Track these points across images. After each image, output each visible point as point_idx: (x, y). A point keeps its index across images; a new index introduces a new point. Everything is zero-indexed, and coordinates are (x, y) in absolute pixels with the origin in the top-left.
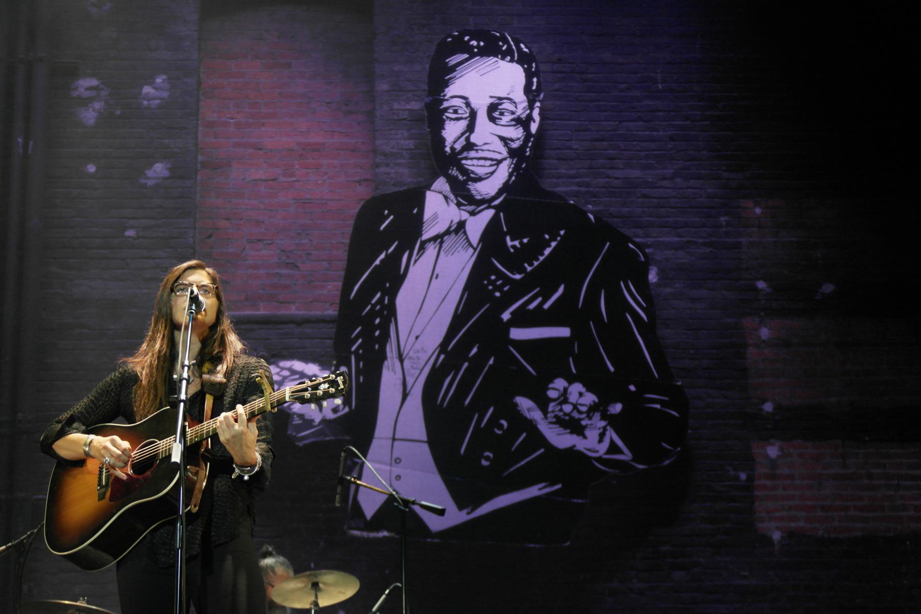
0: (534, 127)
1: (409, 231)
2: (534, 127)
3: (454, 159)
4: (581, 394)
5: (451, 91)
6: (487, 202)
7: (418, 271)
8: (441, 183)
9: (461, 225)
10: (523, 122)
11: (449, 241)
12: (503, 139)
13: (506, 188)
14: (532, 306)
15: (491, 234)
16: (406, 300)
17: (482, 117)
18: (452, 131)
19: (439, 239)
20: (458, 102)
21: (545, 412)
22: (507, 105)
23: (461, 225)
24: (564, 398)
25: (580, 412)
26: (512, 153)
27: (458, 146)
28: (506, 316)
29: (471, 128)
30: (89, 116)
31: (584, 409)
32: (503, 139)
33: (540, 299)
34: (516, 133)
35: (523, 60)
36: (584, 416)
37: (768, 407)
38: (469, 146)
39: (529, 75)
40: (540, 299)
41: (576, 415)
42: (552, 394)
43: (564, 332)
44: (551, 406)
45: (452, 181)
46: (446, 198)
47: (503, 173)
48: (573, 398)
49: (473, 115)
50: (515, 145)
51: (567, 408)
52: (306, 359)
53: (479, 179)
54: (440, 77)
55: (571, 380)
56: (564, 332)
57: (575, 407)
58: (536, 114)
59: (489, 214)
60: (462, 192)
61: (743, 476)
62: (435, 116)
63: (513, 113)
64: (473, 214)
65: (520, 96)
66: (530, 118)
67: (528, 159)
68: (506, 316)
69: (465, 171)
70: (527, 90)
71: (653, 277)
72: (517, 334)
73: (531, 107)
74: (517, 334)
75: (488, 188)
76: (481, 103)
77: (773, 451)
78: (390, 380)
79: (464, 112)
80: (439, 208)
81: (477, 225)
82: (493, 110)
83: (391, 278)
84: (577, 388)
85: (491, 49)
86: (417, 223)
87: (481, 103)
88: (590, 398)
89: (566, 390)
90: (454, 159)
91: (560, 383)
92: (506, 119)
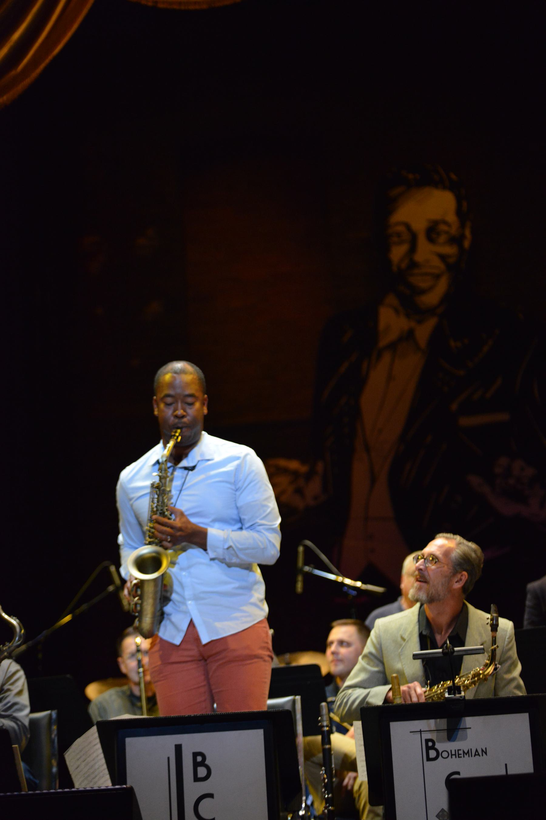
0: (467, 244)
2: (467, 244)
6: (431, 311)
7: (377, 376)
8: (392, 299)
16: (369, 399)
18: (398, 253)
19: (393, 346)
20: (401, 228)
22: (443, 227)
27: (404, 265)
28: (454, 407)
29: (413, 249)
34: (450, 250)
35: (452, 187)
38: (413, 265)
39: (459, 200)
46: (397, 311)
47: (442, 286)
49: (414, 238)
50: (451, 260)
52: (289, 457)
53: (423, 292)
58: (468, 233)
63: (447, 232)
64: (420, 322)
65: (452, 218)
66: (462, 237)
68: (454, 407)
70: (459, 212)
72: (465, 421)
73: (462, 226)
74: (465, 421)
75: (432, 299)
76: (420, 226)
80: (391, 320)
81: (424, 332)
82: (432, 232)
87: (420, 226)
92: (442, 238)
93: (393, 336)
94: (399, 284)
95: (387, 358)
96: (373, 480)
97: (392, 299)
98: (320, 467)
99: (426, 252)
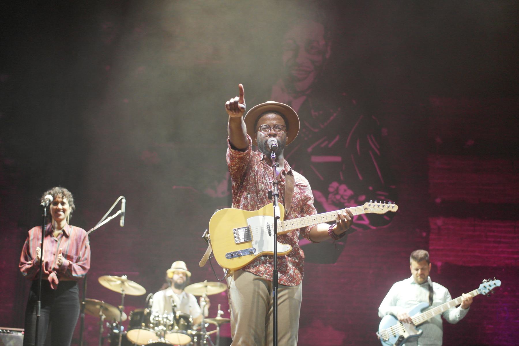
4: (345, 191)
14: (323, 145)
21: (327, 198)
24: (337, 192)
25: (345, 199)
28: (310, 150)
31: (346, 198)
33: (326, 142)
36: (346, 201)
37: (438, 200)
40: (326, 142)
41: (342, 200)
42: (331, 190)
43: (338, 159)
44: (330, 196)
48: (341, 192)
51: (338, 197)
55: (340, 183)
56: (338, 159)
57: (342, 197)
61: (424, 234)
68: (310, 150)
77: (440, 222)
84: (343, 187)
88: (349, 192)
89: (338, 188)
91: (335, 184)
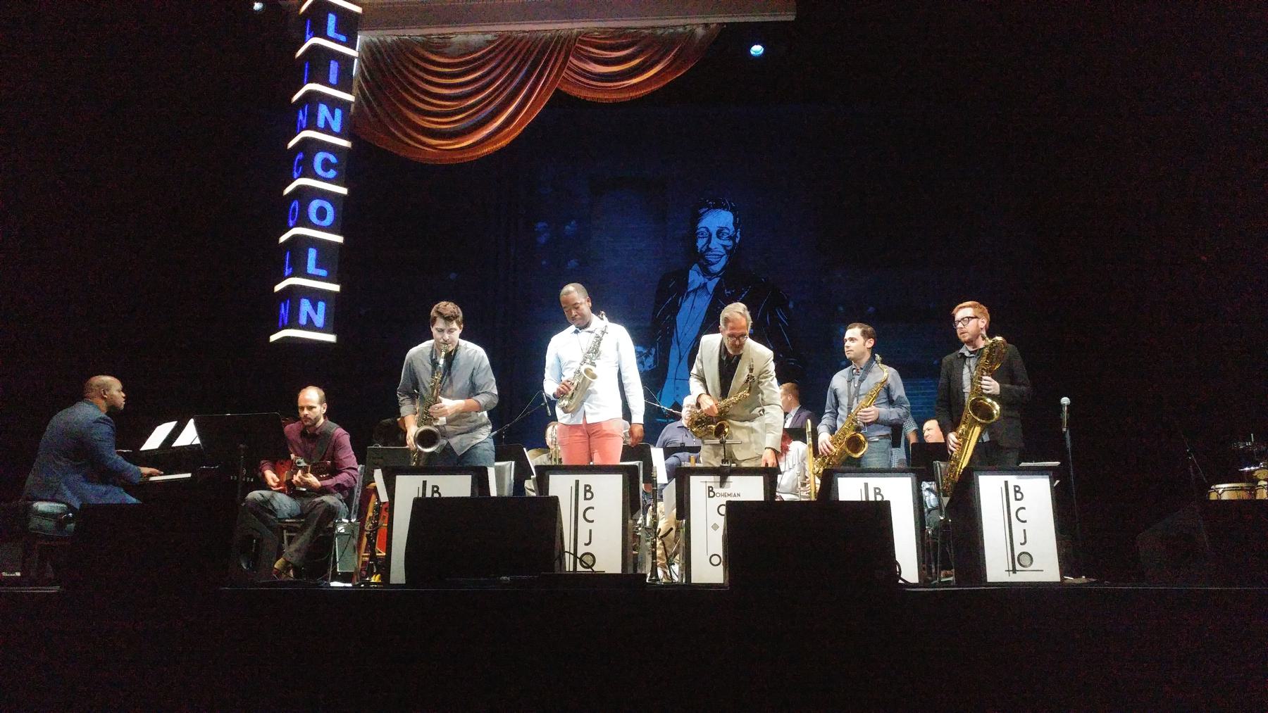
1: (682, 288)
3: (702, 255)
5: (700, 225)
6: (716, 275)
7: (686, 305)
8: (696, 266)
9: (705, 284)
10: (731, 238)
11: (699, 292)
12: (724, 247)
13: (724, 268)
15: (718, 289)
16: (681, 318)
17: (714, 235)
18: (701, 243)
19: (695, 291)
23: (705, 284)
26: (728, 252)
29: (709, 241)
30: (543, 239)
32: (724, 247)
35: (733, 210)
38: (709, 249)
45: (700, 265)
47: (723, 262)
49: (710, 235)
54: (697, 218)
59: (717, 280)
60: (705, 271)
62: (693, 235)
65: (731, 227)
67: (733, 254)
69: (707, 261)
70: (734, 224)
71: (791, 306)
75: (717, 268)
76: (714, 230)
78: (674, 353)
79: (706, 234)
80: (695, 278)
81: (712, 285)
82: (720, 233)
83: (675, 309)
85: (719, 206)
86: (686, 284)
87: (714, 230)
90: (702, 255)
93: (696, 286)
94: (702, 261)
95: (692, 297)
96: (680, 359)
97: (696, 266)
98: (653, 351)
99: (716, 244)
